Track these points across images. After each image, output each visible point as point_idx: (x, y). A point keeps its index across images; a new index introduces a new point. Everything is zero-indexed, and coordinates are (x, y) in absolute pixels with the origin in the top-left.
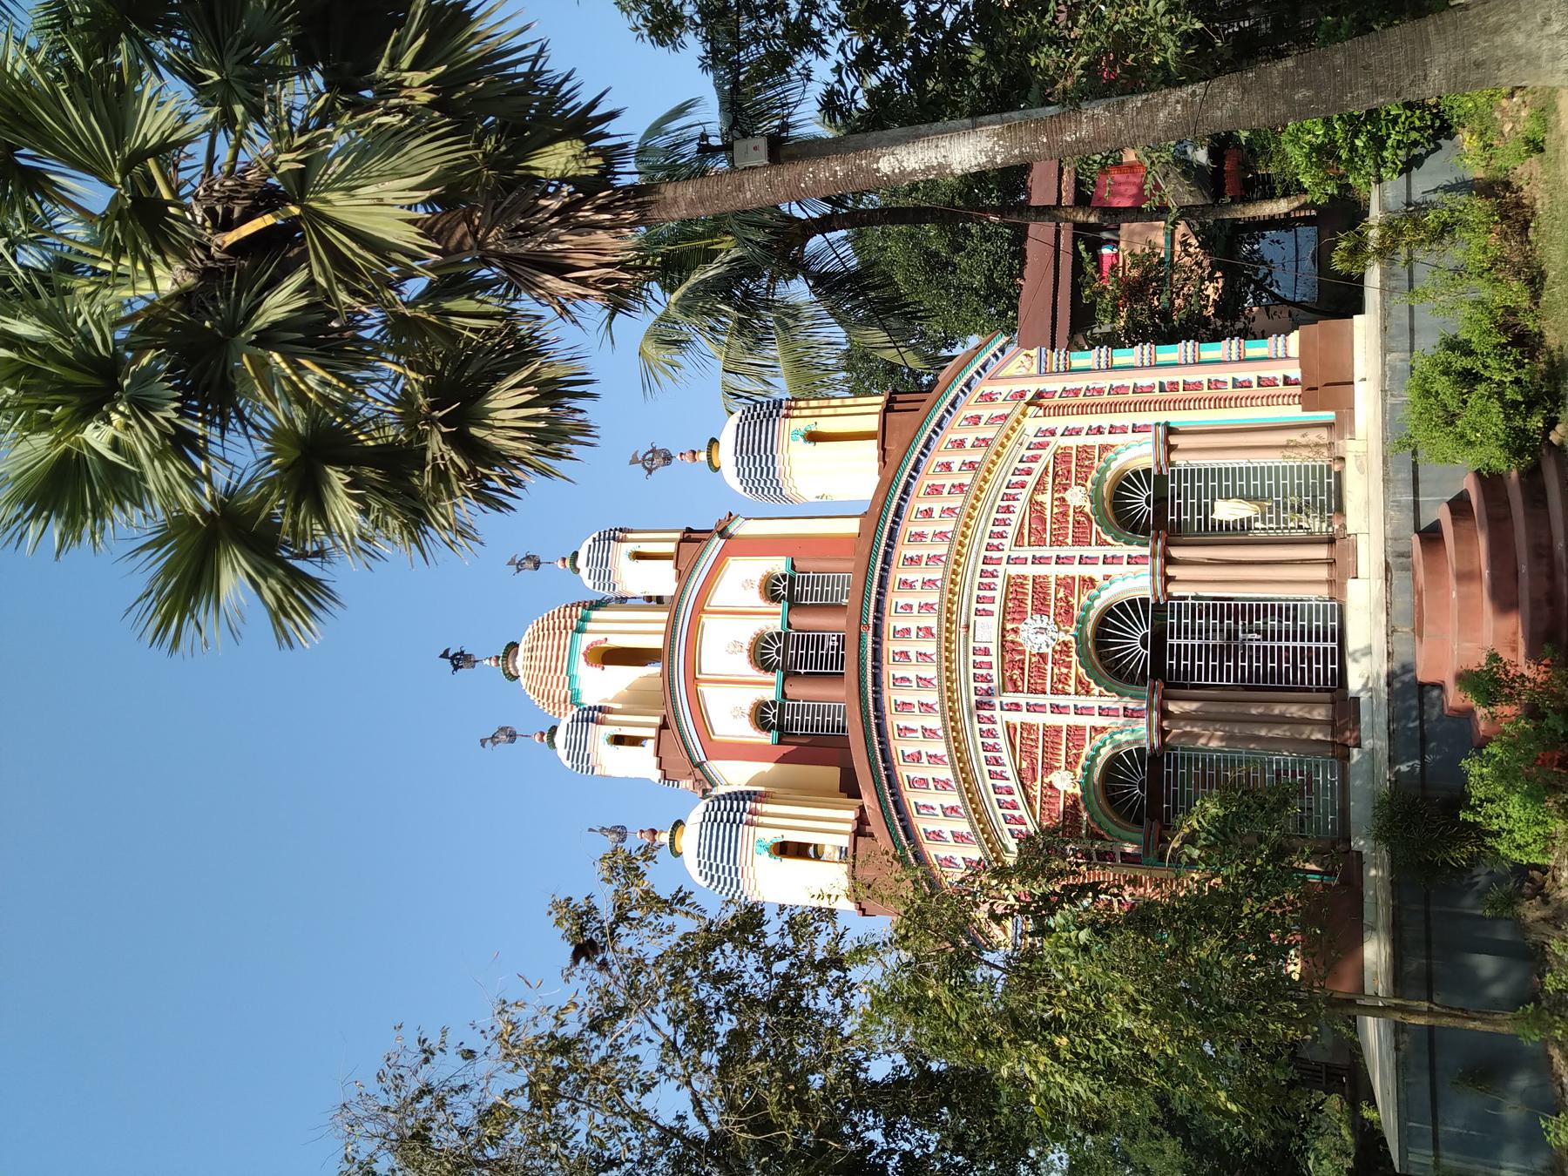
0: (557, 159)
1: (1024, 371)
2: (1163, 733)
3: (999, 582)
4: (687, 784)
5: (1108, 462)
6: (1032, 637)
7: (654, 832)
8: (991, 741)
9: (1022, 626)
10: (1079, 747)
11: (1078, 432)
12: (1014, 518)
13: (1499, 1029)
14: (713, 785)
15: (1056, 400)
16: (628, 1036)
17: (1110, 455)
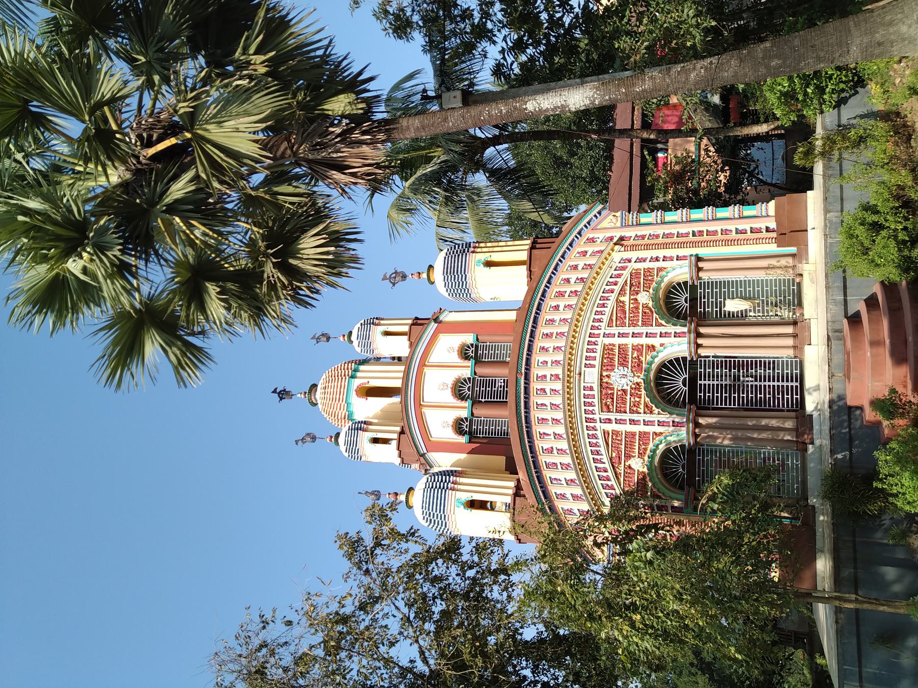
0: (339, 105)
1: (613, 225)
2: (696, 436)
3: (599, 348)
4: (416, 466)
5: (663, 278)
6: (618, 380)
7: (396, 494)
8: (594, 441)
9: (612, 374)
10: (647, 444)
11: (644, 260)
12: (607, 310)
14: (431, 467)
15: (632, 242)
16: (381, 614)
17: (664, 273)
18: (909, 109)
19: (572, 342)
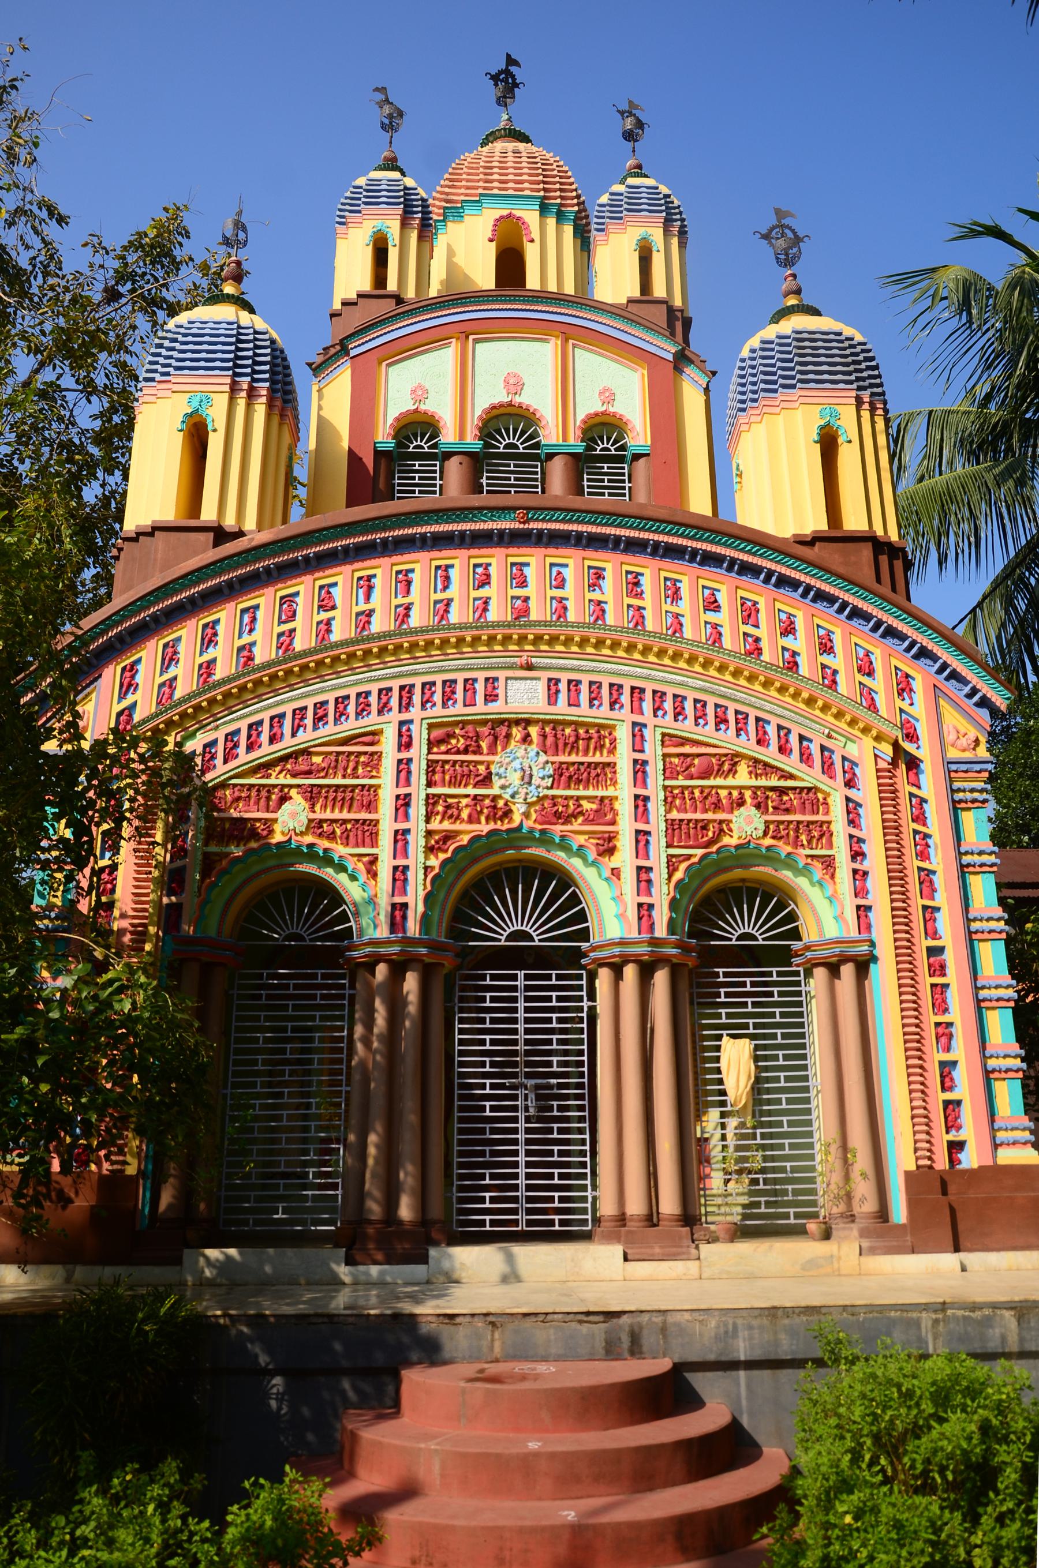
1: (950, 737)
3: (602, 713)
5: (805, 871)
6: (516, 764)
8: (351, 709)
9: (534, 748)
11: (853, 822)
12: (707, 732)
15: (905, 788)
17: (818, 870)
19: (615, 645)
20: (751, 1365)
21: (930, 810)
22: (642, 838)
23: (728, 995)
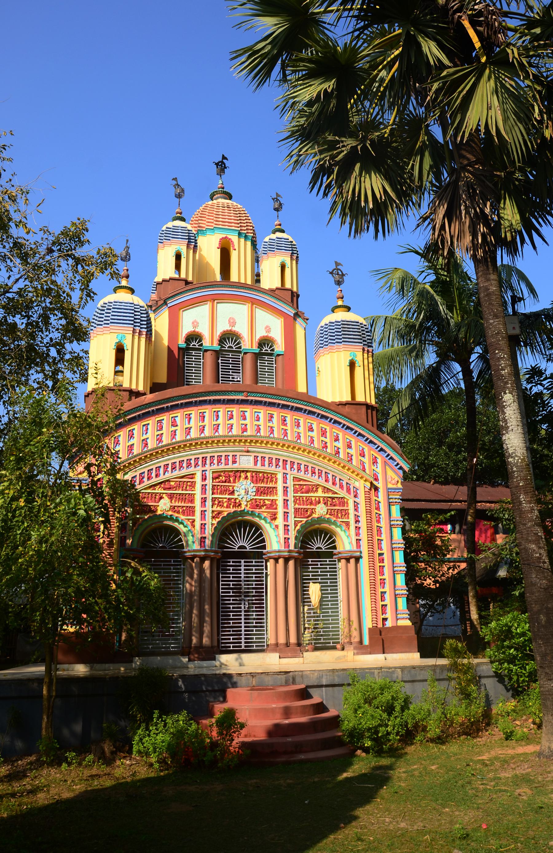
0: (510, 214)
2: (192, 558)
3: (273, 469)
4: (154, 296)
5: (340, 526)
6: (243, 487)
7: (127, 277)
8: (185, 465)
9: (249, 481)
10: (183, 513)
11: (356, 510)
12: (308, 477)
13: (44, 730)
14: (154, 311)
16: (11, 265)
18: (493, 733)
19: (278, 444)
20: (327, 686)
21: (381, 505)
22: (286, 514)
23: (312, 568)
